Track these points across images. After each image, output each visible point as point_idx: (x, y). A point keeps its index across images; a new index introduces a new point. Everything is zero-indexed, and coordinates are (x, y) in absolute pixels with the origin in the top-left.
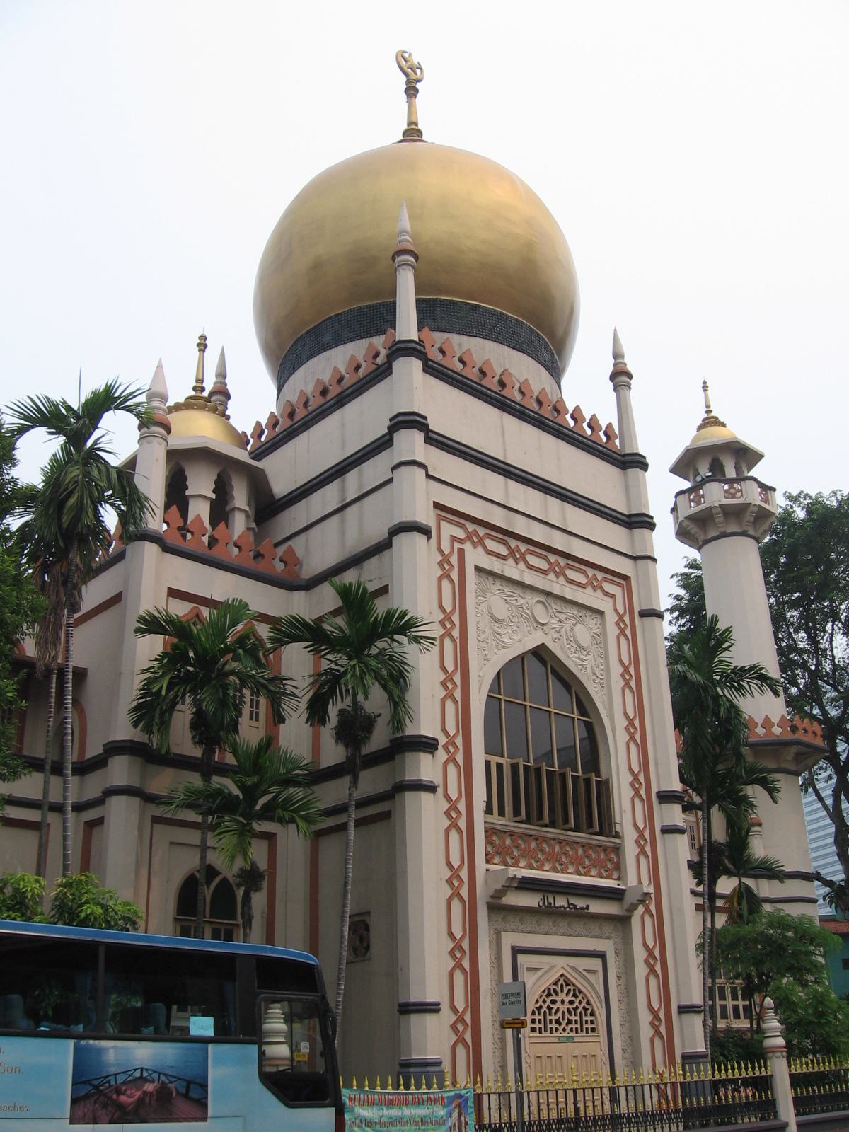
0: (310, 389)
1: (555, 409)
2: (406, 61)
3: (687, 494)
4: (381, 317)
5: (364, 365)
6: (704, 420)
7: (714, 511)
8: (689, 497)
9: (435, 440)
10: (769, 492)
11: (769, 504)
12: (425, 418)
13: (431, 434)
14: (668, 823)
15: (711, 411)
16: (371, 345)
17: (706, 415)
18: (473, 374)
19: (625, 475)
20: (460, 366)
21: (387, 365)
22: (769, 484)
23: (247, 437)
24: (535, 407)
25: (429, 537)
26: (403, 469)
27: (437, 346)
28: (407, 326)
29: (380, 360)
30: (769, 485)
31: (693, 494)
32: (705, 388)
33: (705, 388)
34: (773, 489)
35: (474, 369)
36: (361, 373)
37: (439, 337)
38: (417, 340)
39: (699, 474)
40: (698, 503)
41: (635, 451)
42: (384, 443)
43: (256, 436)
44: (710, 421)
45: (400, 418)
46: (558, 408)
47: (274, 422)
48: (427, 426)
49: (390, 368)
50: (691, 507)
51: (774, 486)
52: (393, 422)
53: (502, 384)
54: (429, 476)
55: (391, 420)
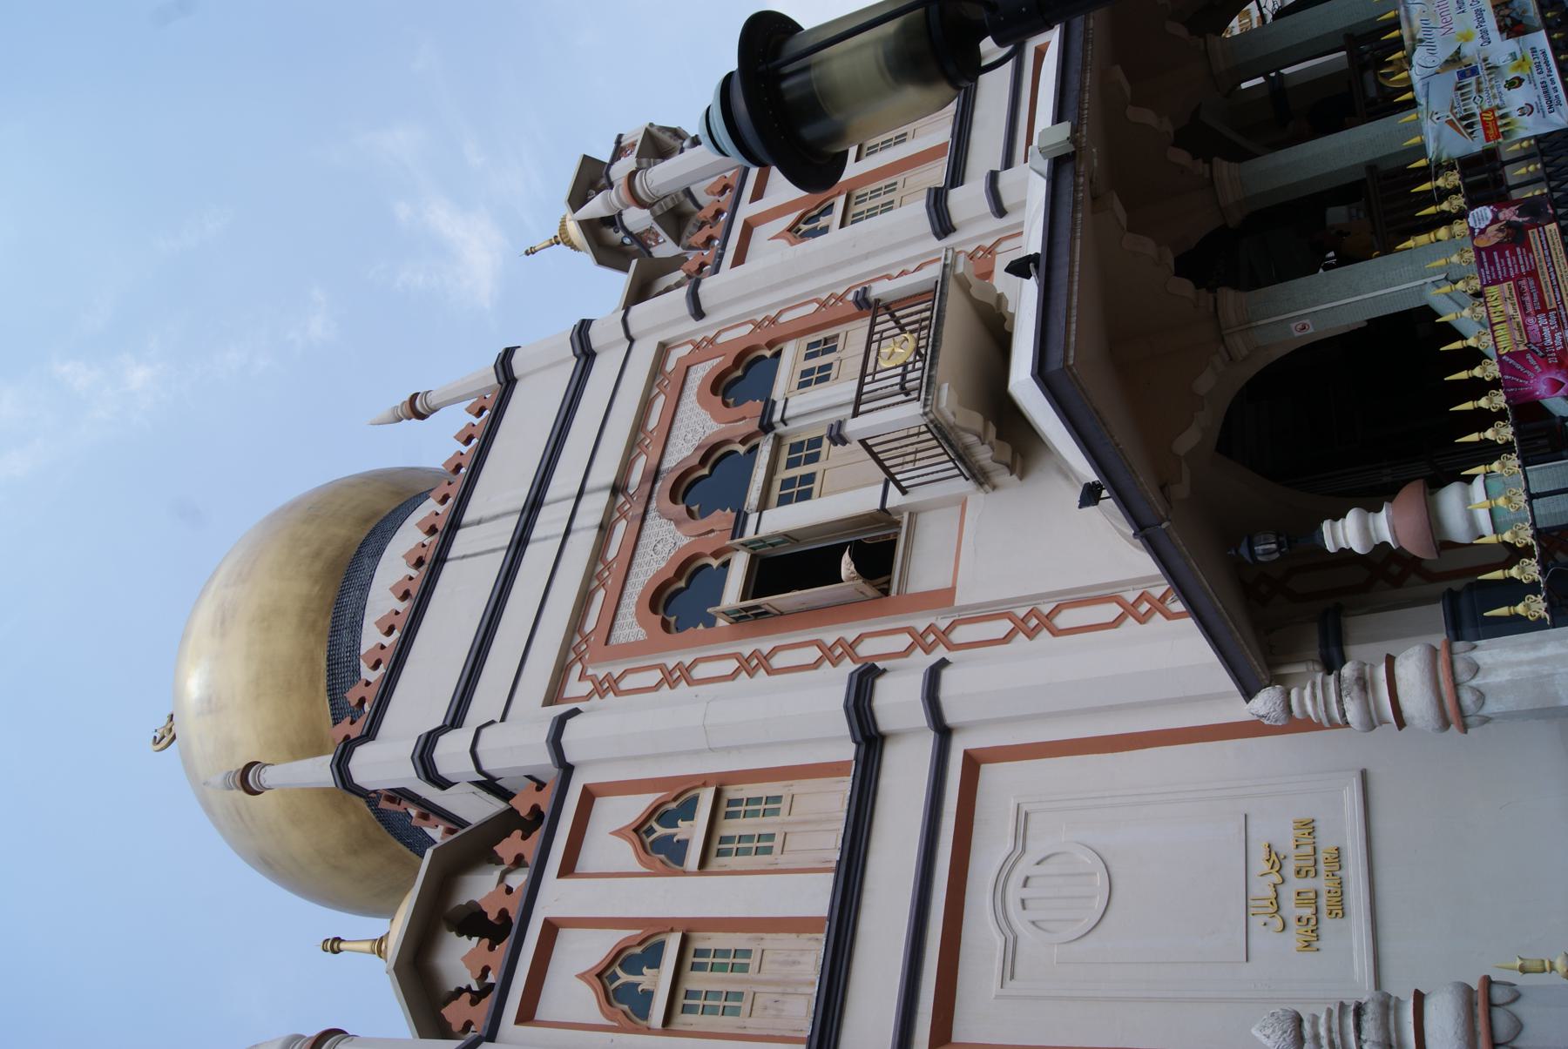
2: (163, 737)
3: (651, 250)
6: (565, 244)
7: (659, 213)
8: (653, 246)
10: (622, 145)
11: (637, 141)
12: (420, 737)
14: (985, 206)
15: (556, 237)
17: (561, 244)
19: (525, 375)
22: (612, 146)
25: (575, 712)
30: (613, 145)
31: (649, 242)
32: (531, 252)
33: (531, 252)
34: (618, 142)
39: (622, 242)
40: (657, 235)
41: (493, 370)
44: (562, 239)
50: (664, 241)
51: (614, 138)
54: (503, 719)
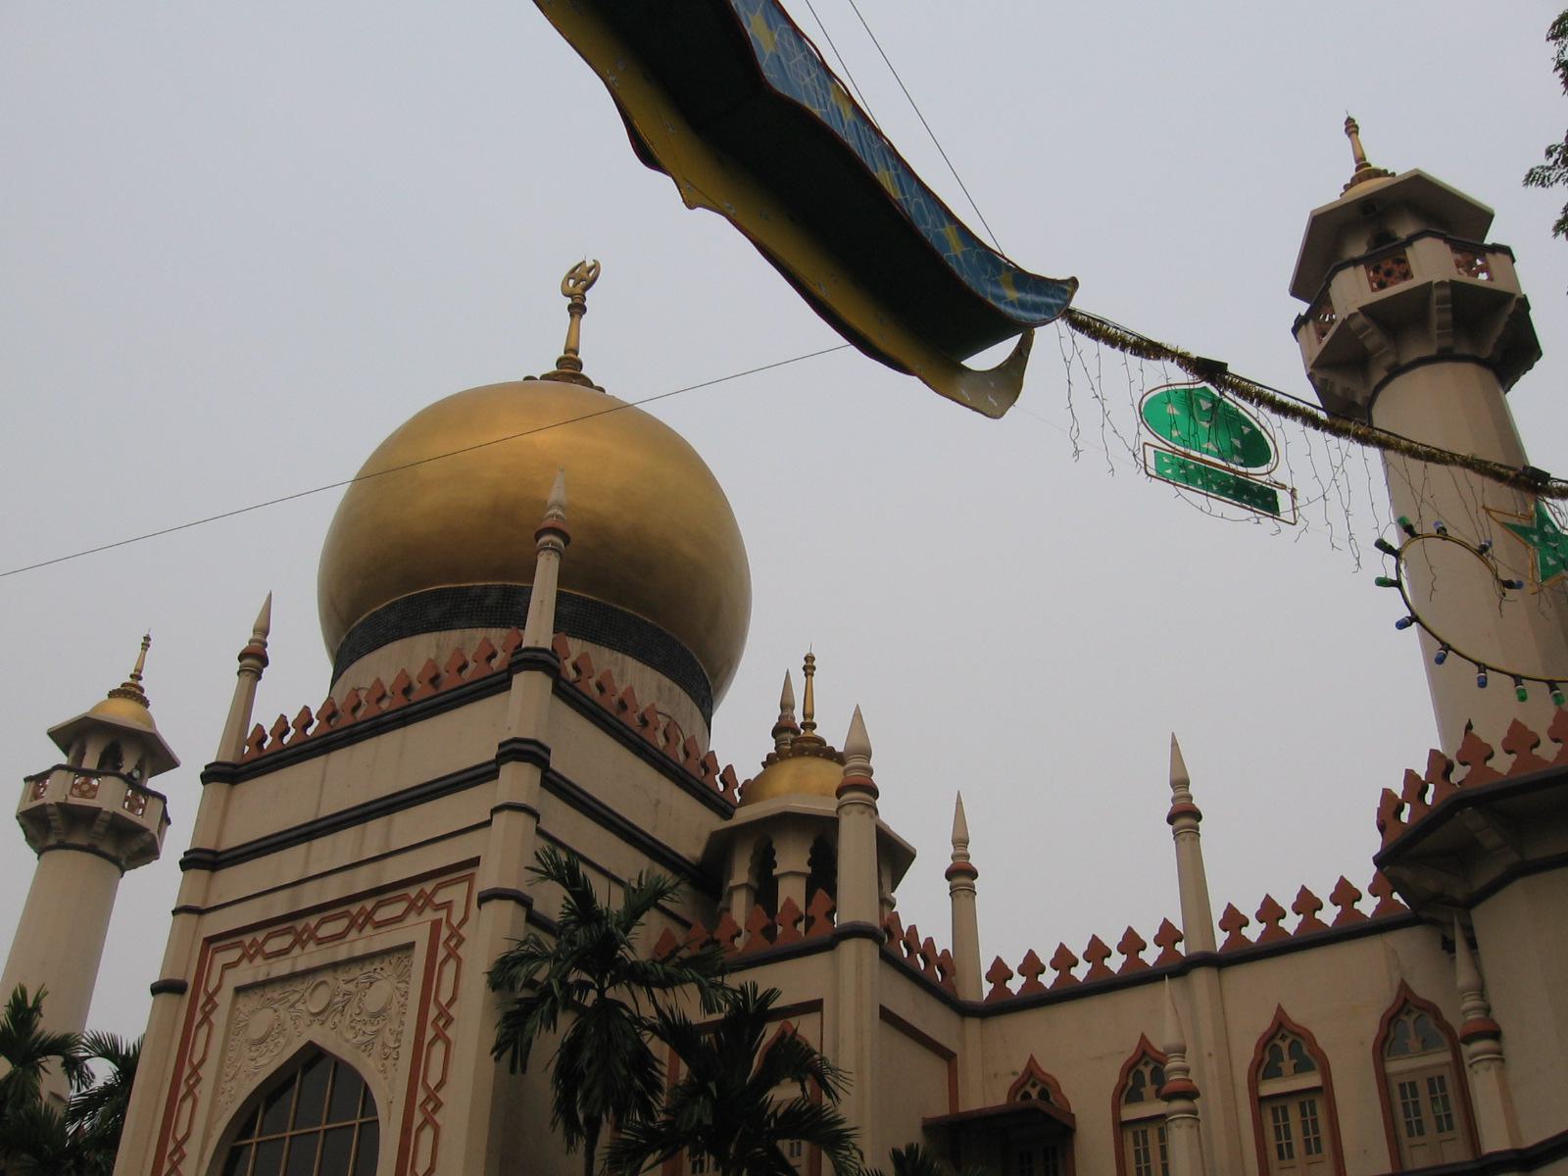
0: (389, 680)
1: (704, 765)
4: (510, 609)
5: (472, 666)
9: (555, 785)
13: (549, 774)
16: (486, 640)
18: (609, 703)
20: (596, 691)
21: (505, 675)
23: (287, 723)
24: (682, 757)
26: (505, 814)
27: (574, 657)
28: (538, 630)
29: (495, 663)
35: (612, 698)
36: (467, 675)
37: (576, 647)
38: (550, 648)
42: (484, 774)
43: (300, 726)
45: (515, 746)
46: (709, 763)
47: (329, 712)
48: (547, 762)
49: (510, 679)
52: (502, 750)
53: (644, 722)
55: (501, 746)
